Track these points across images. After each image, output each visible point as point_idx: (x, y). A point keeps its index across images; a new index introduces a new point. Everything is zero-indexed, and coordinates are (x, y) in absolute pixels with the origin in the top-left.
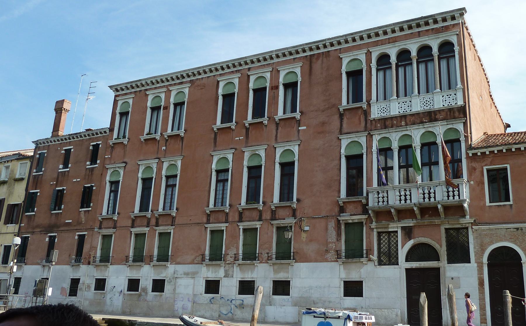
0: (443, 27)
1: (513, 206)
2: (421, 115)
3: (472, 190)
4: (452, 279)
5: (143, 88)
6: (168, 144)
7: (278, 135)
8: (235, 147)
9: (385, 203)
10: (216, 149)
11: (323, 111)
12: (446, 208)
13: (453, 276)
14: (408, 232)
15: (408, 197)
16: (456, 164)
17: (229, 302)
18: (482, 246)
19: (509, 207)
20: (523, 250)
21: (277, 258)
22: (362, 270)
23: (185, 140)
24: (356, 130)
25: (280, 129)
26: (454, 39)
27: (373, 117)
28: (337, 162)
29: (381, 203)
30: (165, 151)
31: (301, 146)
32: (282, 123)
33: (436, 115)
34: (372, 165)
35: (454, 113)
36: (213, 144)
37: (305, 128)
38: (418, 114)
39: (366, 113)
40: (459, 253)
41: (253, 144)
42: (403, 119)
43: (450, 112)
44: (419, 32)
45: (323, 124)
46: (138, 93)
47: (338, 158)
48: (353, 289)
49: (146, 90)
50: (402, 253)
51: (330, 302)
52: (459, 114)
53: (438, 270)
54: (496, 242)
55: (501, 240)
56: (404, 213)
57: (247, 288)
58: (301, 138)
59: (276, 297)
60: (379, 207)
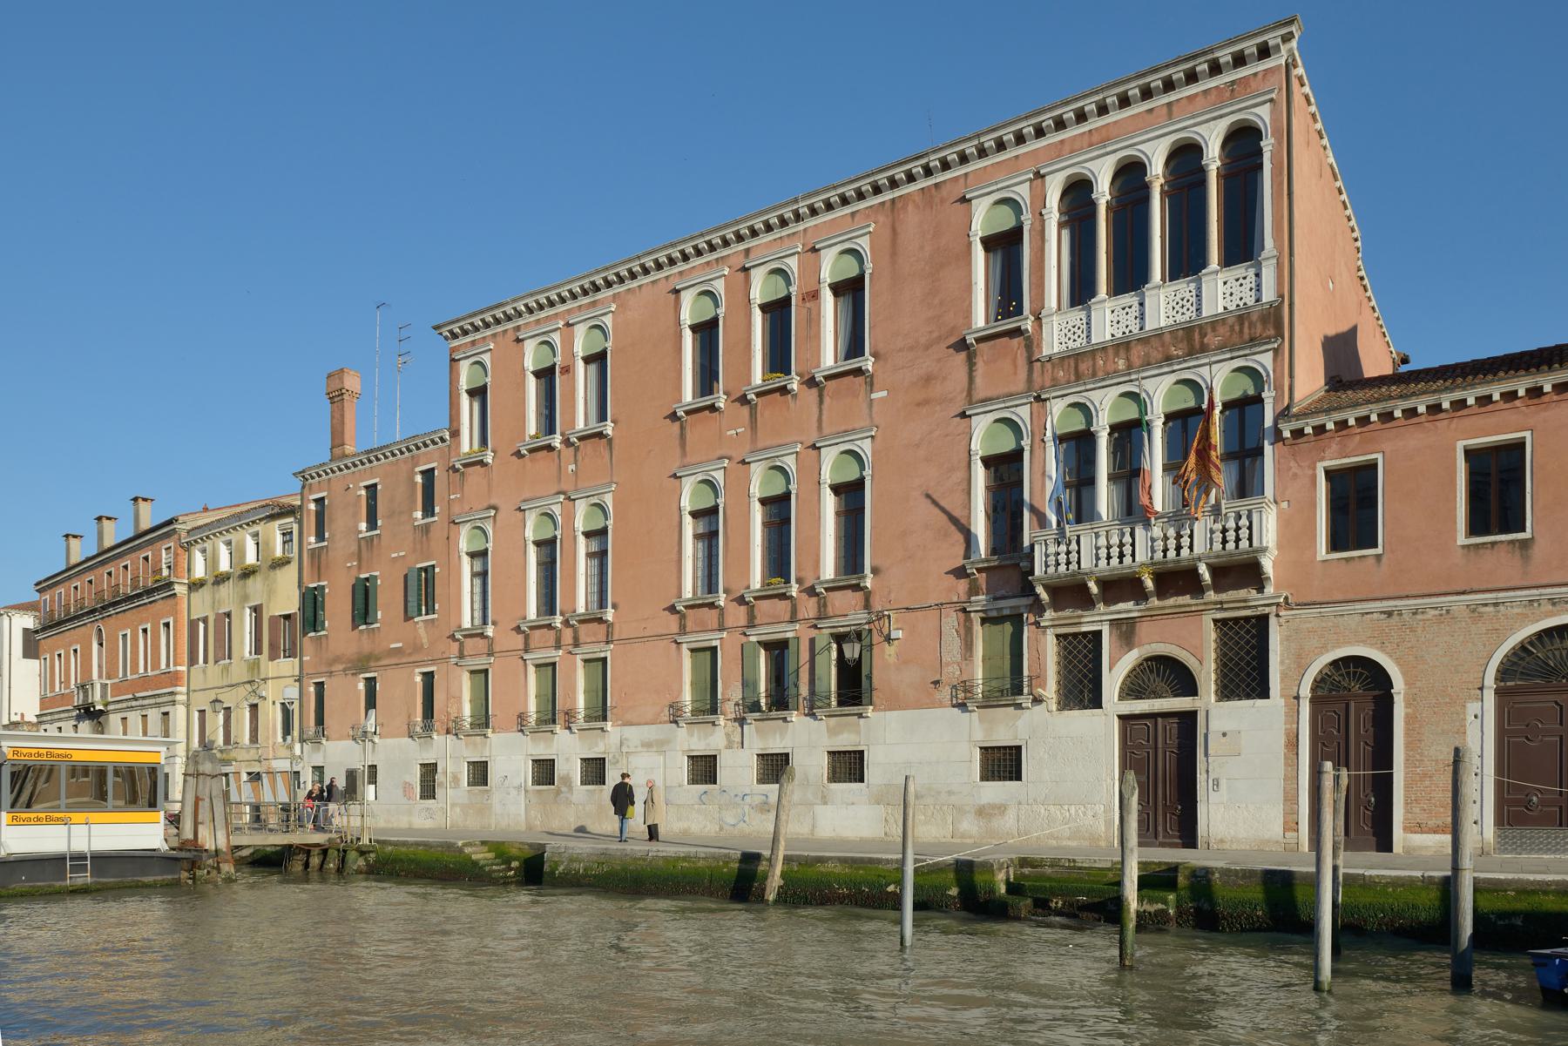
0: (1233, 82)
1: (1384, 559)
2: (1167, 338)
3: (1284, 523)
4: (1224, 735)
5: (510, 325)
6: (579, 458)
7: (824, 417)
8: (729, 453)
9: (1074, 566)
10: (688, 460)
11: (927, 347)
12: (1104, 584)
13: (1225, 729)
14: (1126, 631)
15: (1127, 550)
16: (1248, 461)
17: (738, 799)
18: (1299, 656)
19: (1372, 561)
20: (1398, 664)
21: (840, 704)
22: (1020, 723)
23: (615, 443)
24: (1006, 390)
25: (827, 400)
26: (1262, 115)
27: (1046, 352)
28: (960, 475)
29: (1062, 568)
30: (575, 473)
31: (878, 439)
32: (832, 384)
33: (1203, 335)
34: (1045, 476)
35: (1251, 325)
36: (678, 450)
37: (884, 393)
38: (1159, 335)
39: (1031, 344)
40: (1246, 674)
41: (768, 443)
42: (1122, 353)
43: (1242, 325)
44: (1169, 104)
45: (928, 379)
46: (499, 339)
47: (964, 464)
48: (1003, 763)
49: (518, 328)
50: (1113, 680)
51: (950, 793)
52: (1264, 329)
53: (1188, 720)
54: (1334, 647)
55: (1349, 643)
56: (1121, 587)
57: (775, 767)
58: (877, 420)
59: (834, 786)
60: (1059, 577)
